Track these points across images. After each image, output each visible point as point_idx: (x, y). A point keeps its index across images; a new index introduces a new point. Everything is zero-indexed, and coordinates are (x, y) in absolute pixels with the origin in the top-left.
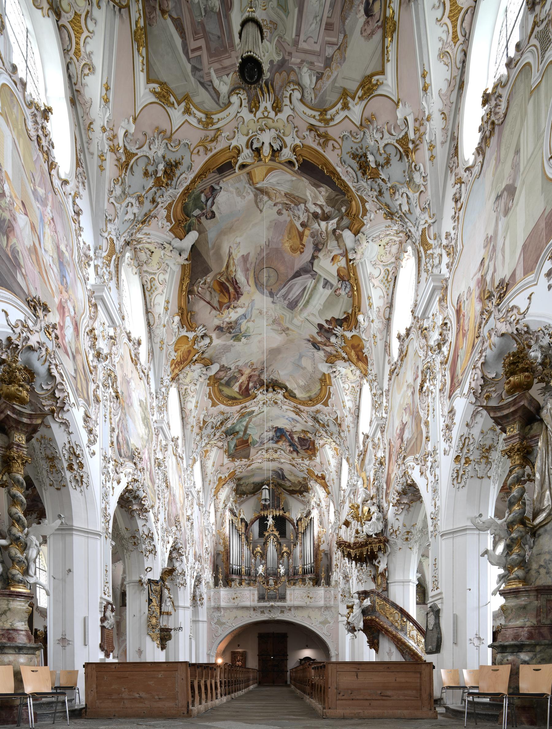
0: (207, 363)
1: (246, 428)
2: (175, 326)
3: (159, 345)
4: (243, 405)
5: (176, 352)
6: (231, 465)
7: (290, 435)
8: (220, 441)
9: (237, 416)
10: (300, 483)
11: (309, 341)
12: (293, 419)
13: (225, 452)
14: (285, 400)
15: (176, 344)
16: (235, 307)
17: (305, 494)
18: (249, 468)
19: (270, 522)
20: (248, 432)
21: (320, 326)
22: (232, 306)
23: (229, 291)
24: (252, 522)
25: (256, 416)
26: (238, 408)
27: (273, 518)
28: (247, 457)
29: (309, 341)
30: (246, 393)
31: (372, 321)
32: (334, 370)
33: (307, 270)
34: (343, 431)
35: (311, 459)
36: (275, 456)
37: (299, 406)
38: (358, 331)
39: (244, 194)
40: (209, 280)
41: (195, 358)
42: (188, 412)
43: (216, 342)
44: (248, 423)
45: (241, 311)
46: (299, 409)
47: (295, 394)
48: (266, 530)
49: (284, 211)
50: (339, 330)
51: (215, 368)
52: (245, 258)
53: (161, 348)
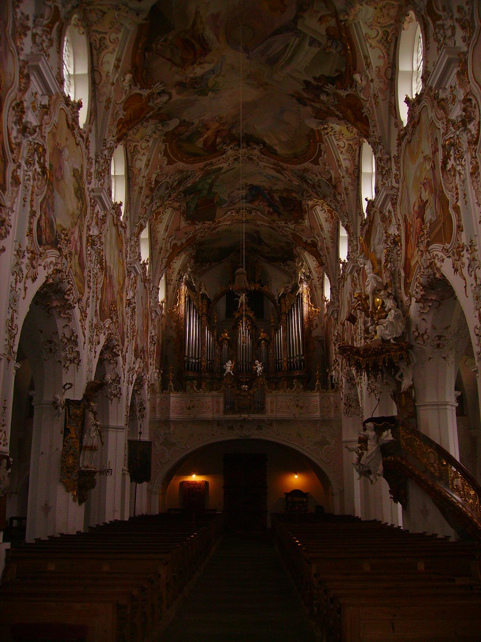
0: (163, 118)
1: (211, 186)
2: (126, 84)
3: (104, 104)
4: (209, 162)
5: (125, 110)
7: (268, 194)
8: (177, 201)
9: (200, 174)
11: (293, 96)
12: (272, 177)
13: (183, 213)
14: (263, 156)
15: (126, 103)
16: (201, 63)
17: (289, 262)
21: (307, 83)
22: (198, 62)
23: (194, 47)
24: (217, 298)
25: (225, 173)
26: (201, 165)
29: (293, 96)
30: (212, 149)
31: (372, 81)
32: (326, 126)
33: (291, 28)
34: (340, 194)
35: (297, 222)
37: (281, 164)
38: (354, 89)
40: (170, 38)
41: (148, 115)
42: (136, 172)
43: (176, 97)
45: (208, 67)
46: (281, 166)
47: (276, 150)
50: (330, 88)
51: (173, 124)
53: (107, 108)
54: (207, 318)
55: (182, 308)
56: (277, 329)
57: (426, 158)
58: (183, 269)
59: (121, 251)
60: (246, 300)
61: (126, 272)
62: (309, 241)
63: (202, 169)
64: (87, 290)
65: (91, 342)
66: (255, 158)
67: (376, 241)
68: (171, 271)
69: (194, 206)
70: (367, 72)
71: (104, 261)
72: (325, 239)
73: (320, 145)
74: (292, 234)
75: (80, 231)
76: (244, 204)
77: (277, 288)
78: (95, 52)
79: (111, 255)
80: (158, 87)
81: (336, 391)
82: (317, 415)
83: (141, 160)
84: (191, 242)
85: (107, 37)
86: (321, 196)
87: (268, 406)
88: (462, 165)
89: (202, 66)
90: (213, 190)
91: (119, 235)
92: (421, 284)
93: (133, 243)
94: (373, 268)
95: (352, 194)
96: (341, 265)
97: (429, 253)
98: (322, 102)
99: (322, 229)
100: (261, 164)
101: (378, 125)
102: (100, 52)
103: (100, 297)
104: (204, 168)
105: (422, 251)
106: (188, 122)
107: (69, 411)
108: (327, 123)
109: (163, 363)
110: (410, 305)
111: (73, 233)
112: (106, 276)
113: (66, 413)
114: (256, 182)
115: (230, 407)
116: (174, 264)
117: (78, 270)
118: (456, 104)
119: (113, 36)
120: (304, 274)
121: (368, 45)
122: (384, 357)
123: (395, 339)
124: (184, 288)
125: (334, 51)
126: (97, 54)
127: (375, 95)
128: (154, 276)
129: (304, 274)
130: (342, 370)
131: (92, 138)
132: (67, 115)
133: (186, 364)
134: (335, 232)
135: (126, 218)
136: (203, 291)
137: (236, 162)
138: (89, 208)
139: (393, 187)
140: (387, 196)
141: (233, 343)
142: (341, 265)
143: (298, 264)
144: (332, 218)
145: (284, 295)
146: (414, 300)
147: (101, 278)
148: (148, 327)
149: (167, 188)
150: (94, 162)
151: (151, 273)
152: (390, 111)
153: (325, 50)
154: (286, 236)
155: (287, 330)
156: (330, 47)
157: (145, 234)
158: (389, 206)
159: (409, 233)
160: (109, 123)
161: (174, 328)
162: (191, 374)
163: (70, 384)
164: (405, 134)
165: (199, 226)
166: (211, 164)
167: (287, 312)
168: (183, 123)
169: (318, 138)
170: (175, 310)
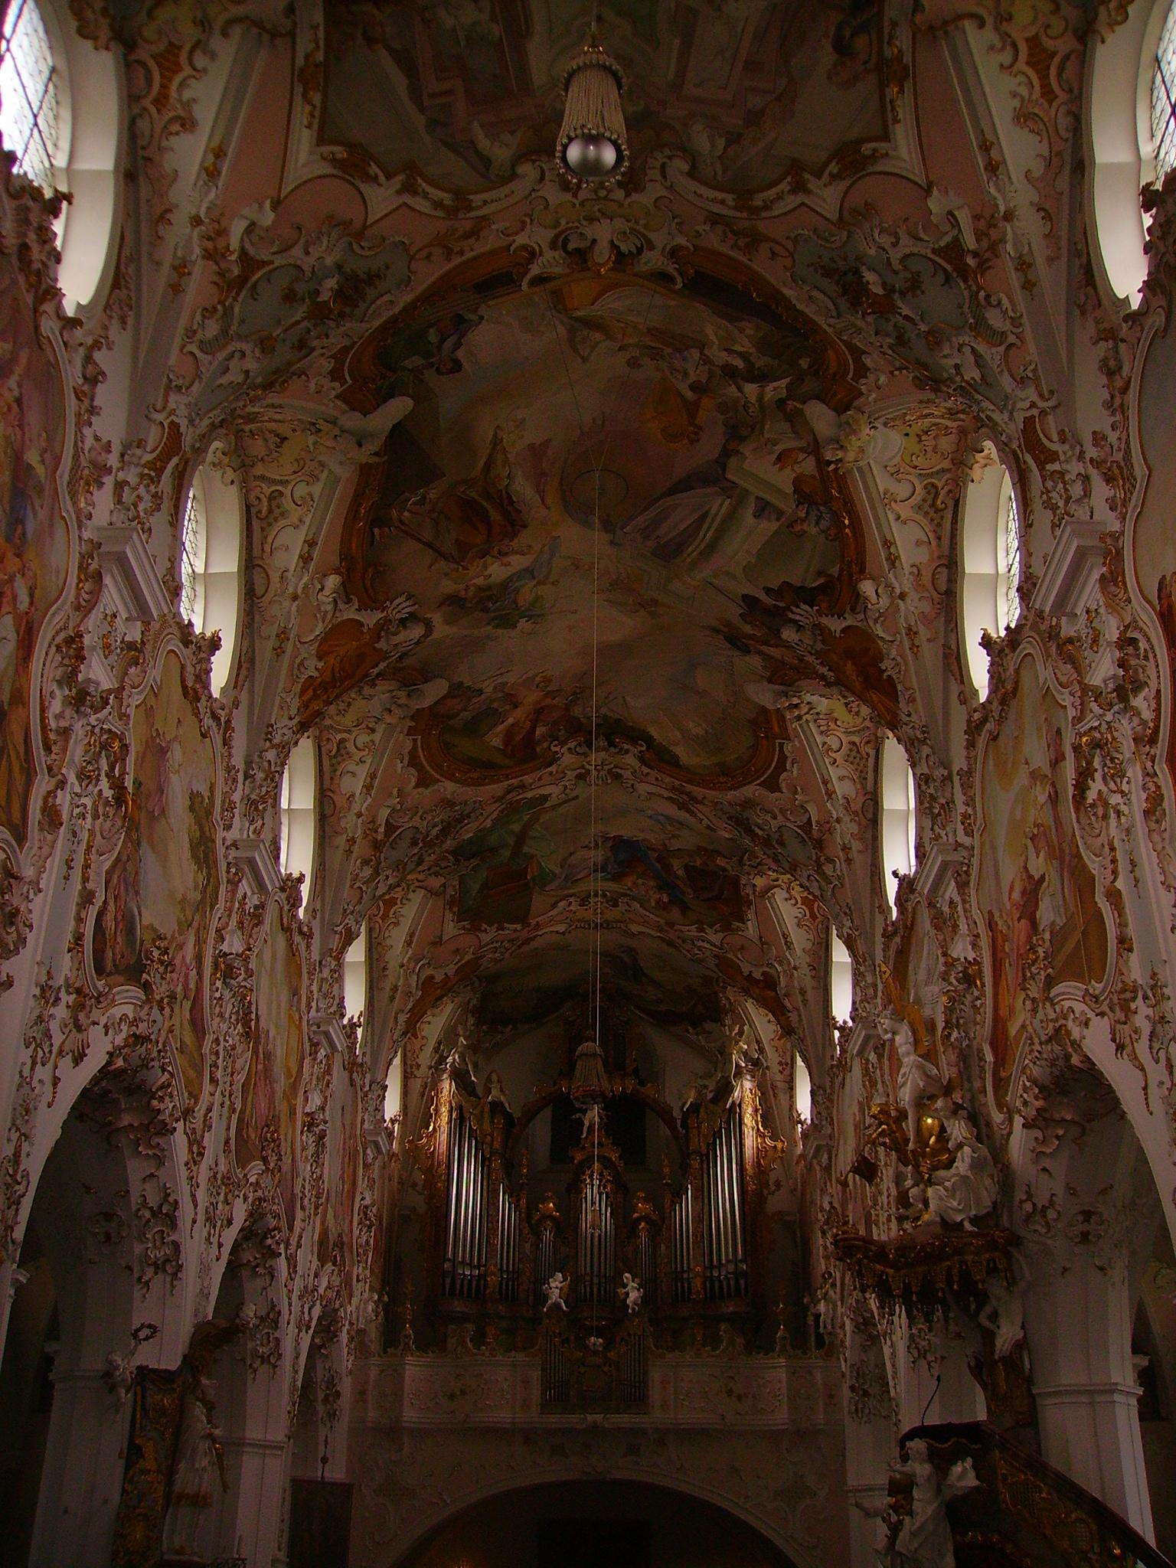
0: (409, 675)
1: (521, 839)
2: (326, 598)
3: (271, 643)
5: (320, 659)
7: (659, 859)
8: (437, 874)
12: (667, 817)
13: (451, 904)
14: (646, 770)
17: (709, 1026)
18: (526, 948)
21: (750, 601)
24: (530, 1114)
25: (553, 808)
26: (497, 789)
28: (522, 918)
29: (718, 631)
30: (525, 752)
31: (902, 597)
32: (795, 701)
33: (713, 476)
35: (726, 928)
36: (612, 914)
37: (689, 787)
39: (542, 329)
41: (376, 671)
43: (442, 630)
44: (527, 827)
45: (518, 562)
46: (688, 794)
49: (646, 361)
50: (803, 613)
51: (433, 692)
52: (537, 452)
53: (279, 651)
54: (503, 1166)
55: (443, 1137)
56: (678, 1194)
57: (1035, 776)
58: (448, 1040)
59: (295, 992)
60: (600, 1118)
61: (307, 1045)
62: (757, 975)
63: (499, 799)
64: (207, 1087)
65: (210, 1220)
66: (627, 774)
67: (922, 975)
68: (417, 1043)
69: (477, 886)
70: (891, 575)
71: (253, 1016)
72: (795, 968)
73: (781, 745)
74: (715, 956)
75: (200, 942)
76: (597, 884)
77: (679, 1090)
78: (256, 525)
79: (270, 1002)
80: (400, 607)
82: (781, 1416)
83: (354, 774)
84: (468, 973)
85: (287, 492)
86: (786, 865)
87: (655, 1393)
88: (1122, 792)
89: (505, 560)
90: (526, 849)
91: (292, 952)
92: (1035, 1082)
93: (326, 973)
94: (916, 1043)
95: (860, 860)
96: (837, 1034)
97: (1053, 1005)
98: (787, 645)
99: (789, 945)
100: (643, 788)
101: (918, 700)
102: (270, 525)
103: (238, 1106)
104: (503, 797)
105: (1034, 1000)
106: (469, 687)
107: (143, 1397)
108: (797, 693)
109: (390, 1276)
110: (1010, 1133)
111: (180, 947)
112: (255, 1052)
113: (135, 1401)
114: (627, 830)
115: (557, 1396)
116: (424, 1026)
117: (189, 1038)
118: (1101, 650)
119: (301, 490)
120: (745, 1054)
121: (891, 517)
122: (949, 1269)
123: (973, 1221)
124: (447, 1087)
125: (813, 530)
126: (263, 529)
127: (909, 629)
128: (375, 1055)
129: (745, 1054)
131: (240, 721)
132: (183, 667)
133: (448, 1280)
134: (822, 953)
135: (312, 911)
136: (495, 1094)
137: (581, 783)
138: (223, 889)
139: (958, 845)
140: (945, 865)
141: (568, 1225)
142: (837, 1034)
143: (731, 1030)
144: (813, 917)
145: (695, 1108)
146: (1018, 1121)
147: (244, 1060)
148: (354, 1184)
149: (414, 843)
150: (241, 777)
151: (368, 1050)
152: (947, 667)
153: (791, 526)
154: (701, 961)
155: (704, 1195)
156: (803, 520)
157: (356, 953)
158: (951, 890)
159: (1000, 955)
160: (281, 686)
161: (419, 1188)
162: (459, 1306)
163: (150, 1326)
164: (984, 721)
165: (489, 934)
166: (523, 787)
167: (705, 1151)
168: (457, 690)
169: (776, 729)
170: (424, 1140)
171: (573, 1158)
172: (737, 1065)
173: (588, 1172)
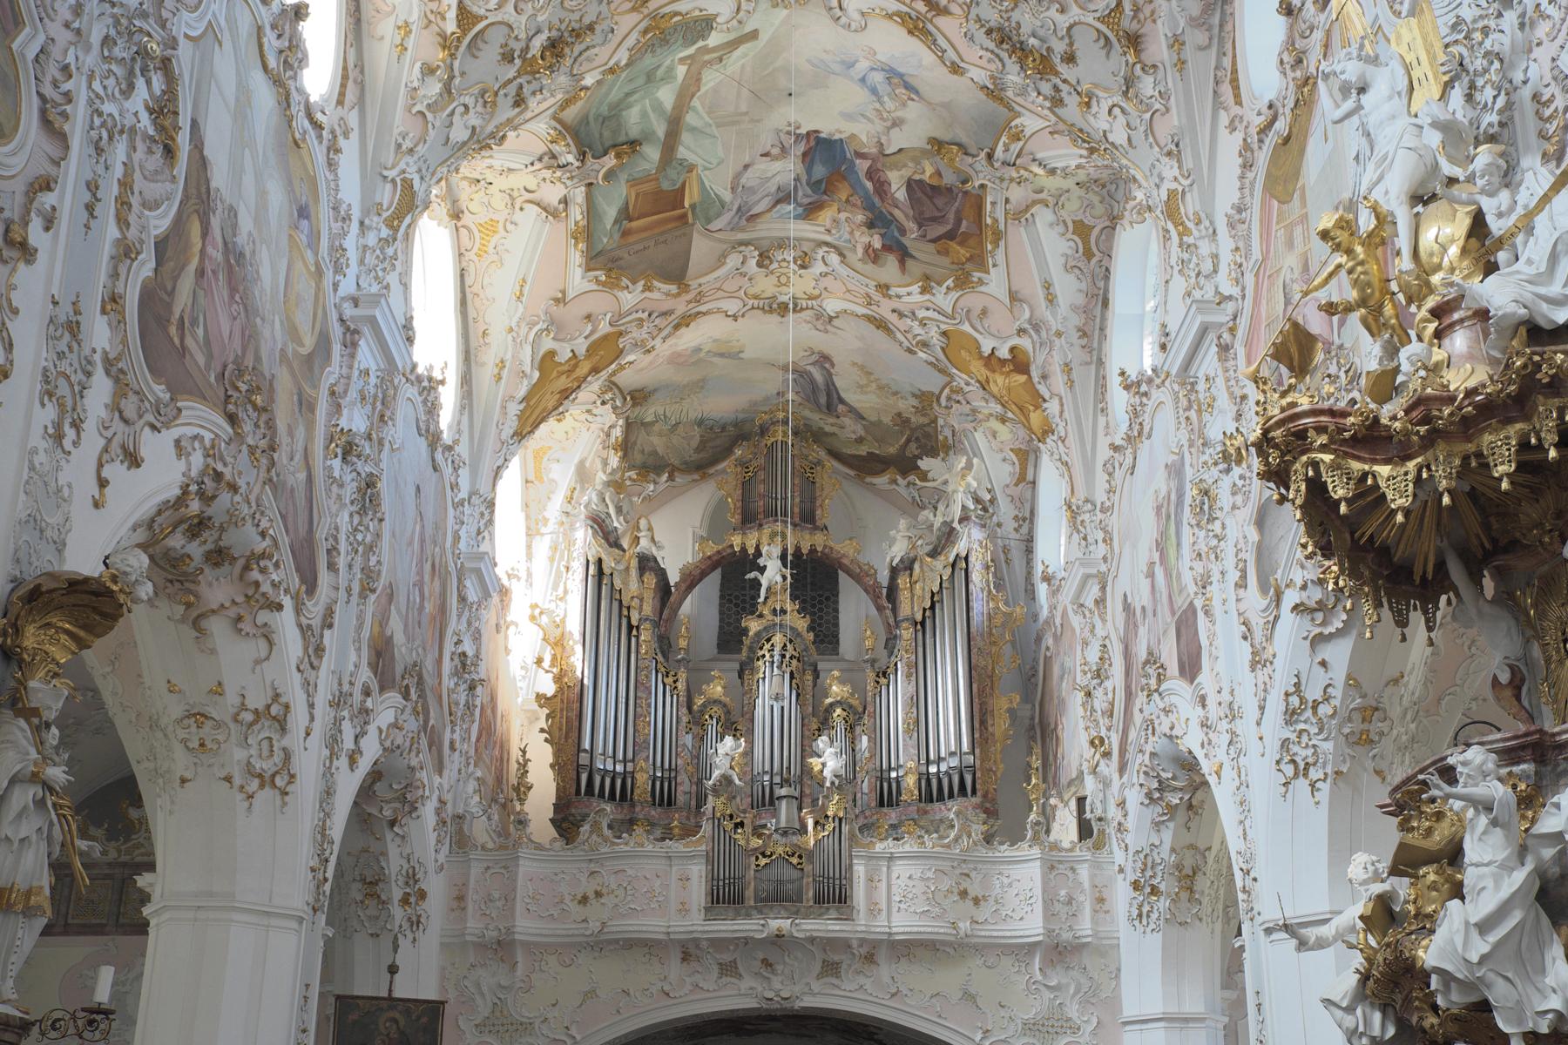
6: (602, 304)
10: (902, 421)
17: (924, 464)
18: (688, 338)
19: (773, 573)
20: (682, 152)
27: (783, 558)
28: (676, 274)
36: (800, 284)
48: (751, 608)
60: (784, 578)
62: (1004, 353)
74: (944, 333)
81: (1098, 846)
84: (606, 350)
130: (1122, 769)
145: (908, 565)
151: (465, 438)
154: (925, 345)
155: (920, 671)
157: (432, 240)
167: (919, 617)
171: (745, 631)
172: (964, 507)
173: (767, 646)
